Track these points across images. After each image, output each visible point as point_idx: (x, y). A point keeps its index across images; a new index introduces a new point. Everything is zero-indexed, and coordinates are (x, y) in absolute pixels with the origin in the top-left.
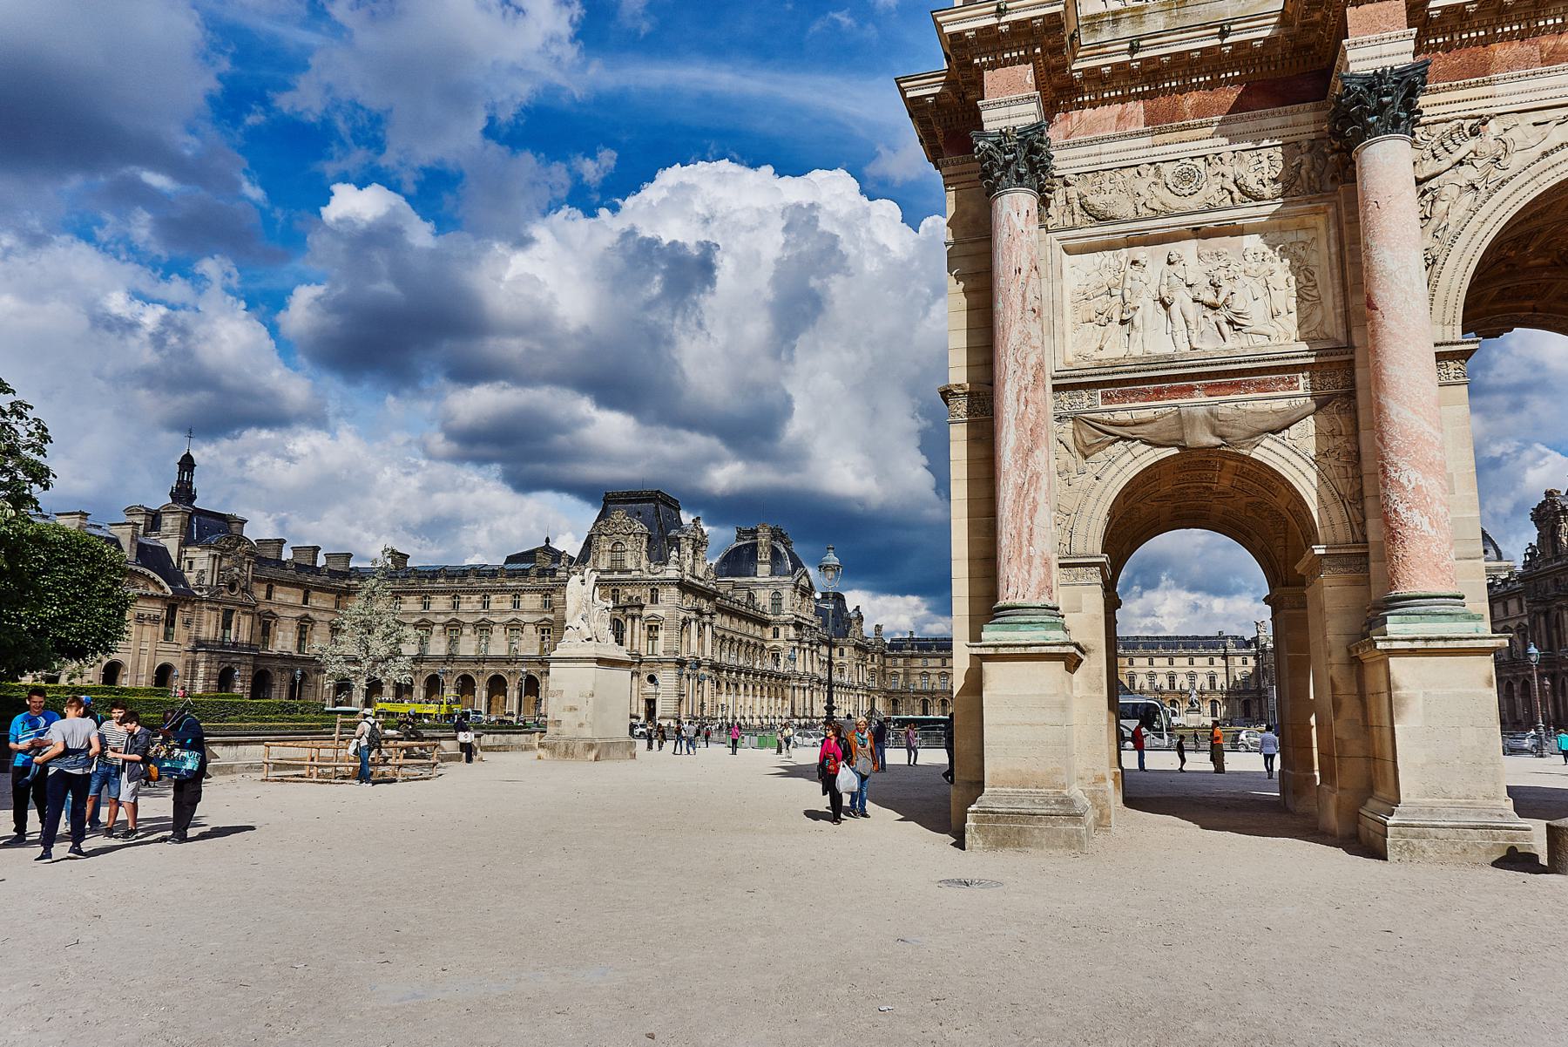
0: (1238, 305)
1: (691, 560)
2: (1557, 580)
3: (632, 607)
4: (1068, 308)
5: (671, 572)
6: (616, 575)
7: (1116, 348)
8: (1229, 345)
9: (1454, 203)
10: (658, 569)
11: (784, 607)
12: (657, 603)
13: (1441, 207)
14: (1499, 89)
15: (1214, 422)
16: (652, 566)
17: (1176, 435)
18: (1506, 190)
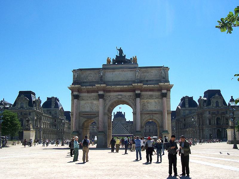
7: (84, 110)
9: (107, 101)
10: (31, 108)
16: (29, 107)
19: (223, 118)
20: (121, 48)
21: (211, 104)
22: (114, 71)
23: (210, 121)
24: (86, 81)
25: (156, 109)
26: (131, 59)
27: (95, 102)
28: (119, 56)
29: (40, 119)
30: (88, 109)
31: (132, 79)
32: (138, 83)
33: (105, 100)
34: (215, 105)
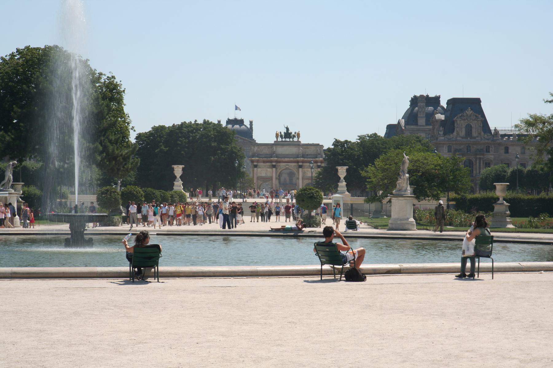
19: (478, 162)
20: (287, 126)
21: (455, 131)
22: (283, 147)
27: (269, 170)
30: (263, 175)
32: (301, 157)
33: (276, 169)
34: (463, 133)
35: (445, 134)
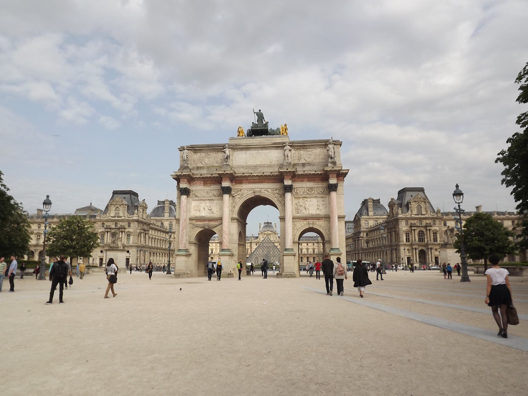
0: (213, 210)
1: (142, 213)
2: (393, 223)
3: (122, 228)
4: (192, 208)
5: (135, 217)
6: (116, 218)
7: (198, 214)
8: (211, 215)
10: (131, 216)
11: (173, 227)
12: (130, 227)
13: (236, 200)
14: (243, 186)
15: (208, 226)
16: (129, 215)
17: (203, 227)
18: (243, 199)
19: (428, 232)
20: (260, 111)
21: (410, 210)
23: (408, 236)
24: (201, 165)
25: (318, 212)
26: (278, 129)
28: (257, 123)
29: (146, 234)
31: (278, 161)
34: (415, 212)
35: (402, 212)
